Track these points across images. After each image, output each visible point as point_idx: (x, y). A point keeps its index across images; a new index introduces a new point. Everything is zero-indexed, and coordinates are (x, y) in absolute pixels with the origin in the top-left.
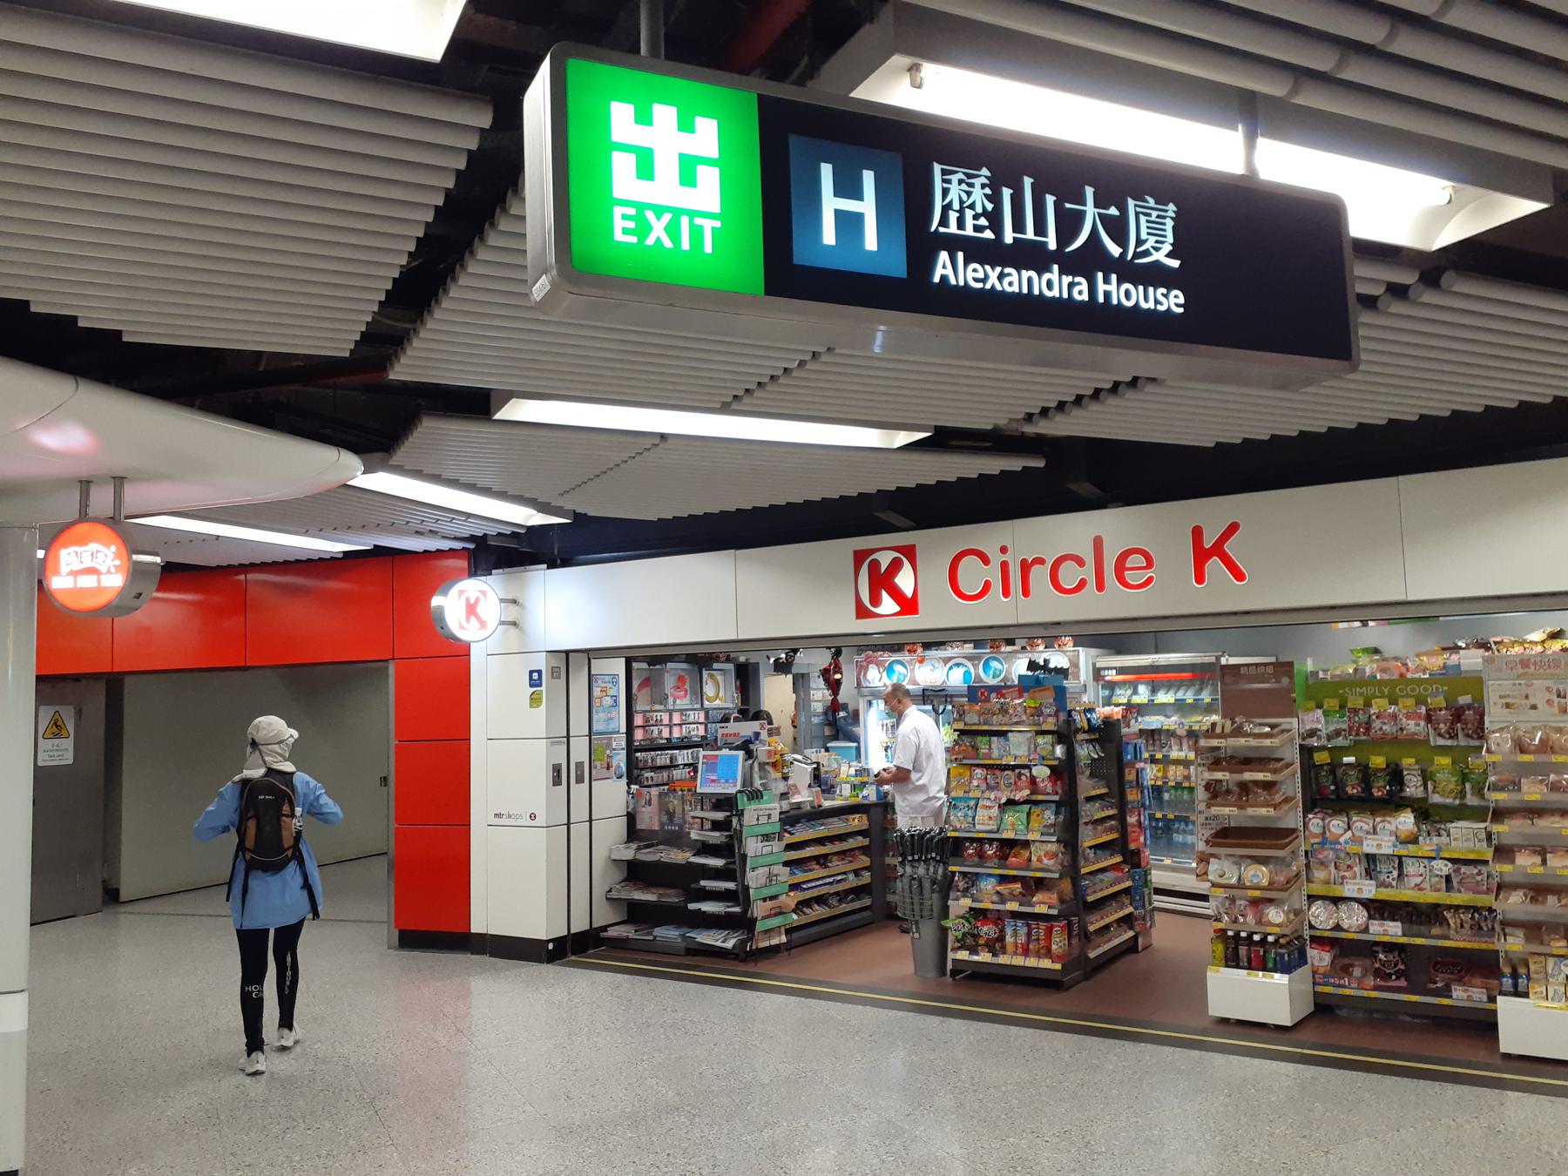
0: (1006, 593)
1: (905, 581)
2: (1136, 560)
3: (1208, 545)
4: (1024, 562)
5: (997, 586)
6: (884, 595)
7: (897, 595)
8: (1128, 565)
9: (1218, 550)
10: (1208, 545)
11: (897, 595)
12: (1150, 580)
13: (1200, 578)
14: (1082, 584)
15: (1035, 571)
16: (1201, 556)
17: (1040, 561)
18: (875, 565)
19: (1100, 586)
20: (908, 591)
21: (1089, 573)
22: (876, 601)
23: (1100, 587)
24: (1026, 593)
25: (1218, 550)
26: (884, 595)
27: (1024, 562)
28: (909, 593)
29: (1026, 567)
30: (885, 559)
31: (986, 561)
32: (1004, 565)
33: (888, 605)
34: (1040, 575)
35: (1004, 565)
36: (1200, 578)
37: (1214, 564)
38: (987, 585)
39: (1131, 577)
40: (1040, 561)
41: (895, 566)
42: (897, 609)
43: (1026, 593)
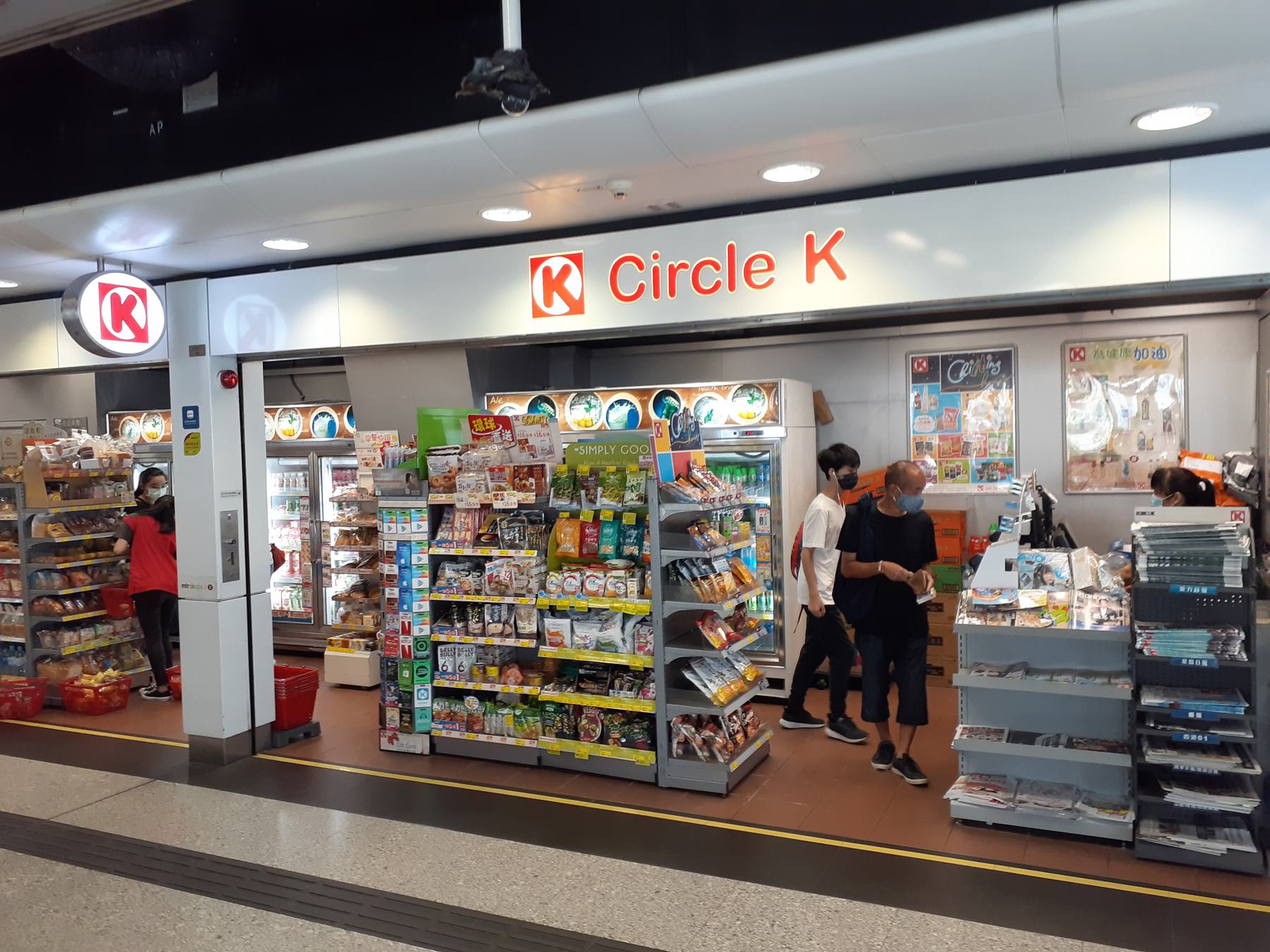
0: (656, 295)
1: (573, 284)
2: (761, 264)
3: (817, 250)
4: (671, 267)
6: (556, 297)
7: (566, 296)
8: (753, 269)
9: (825, 254)
10: (817, 250)
11: (566, 296)
12: (771, 281)
13: (810, 278)
14: (718, 285)
16: (812, 259)
17: (684, 266)
19: (732, 287)
22: (548, 302)
23: (732, 287)
24: (672, 293)
25: (825, 254)
26: (556, 297)
27: (671, 267)
29: (672, 271)
30: (556, 265)
31: (641, 266)
32: (656, 270)
33: (559, 305)
34: (684, 277)
35: (656, 270)
36: (810, 278)
37: (822, 267)
38: (642, 287)
39: (756, 279)
40: (684, 266)
41: (566, 271)
43: (672, 293)
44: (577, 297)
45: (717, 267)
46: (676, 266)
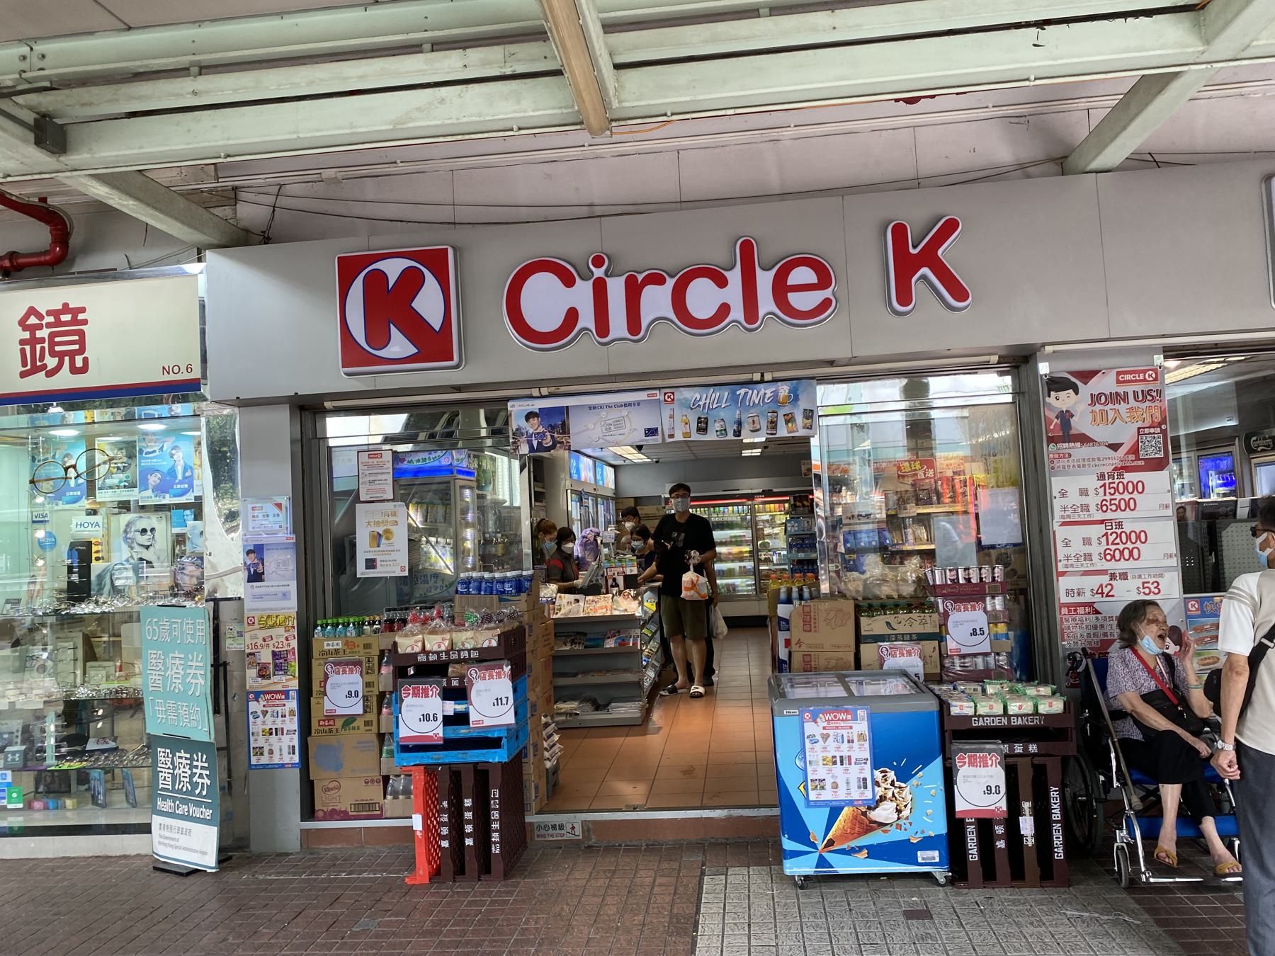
1: (429, 303)
5: (587, 319)
6: (393, 330)
7: (415, 327)
9: (929, 257)
12: (826, 304)
14: (724, 309)
17: (657, 279)
20: (436, 323)
21: (733, 293)
22: (378, 336)
26: (393, 330)
28: (437, 326)
31: (568, 281)
33: (399, 345)
34: (656, 301)
38: (572, 315)
42: (414, 350)
44: (437, 326)
45: (721, 282)
46: (640, 278)
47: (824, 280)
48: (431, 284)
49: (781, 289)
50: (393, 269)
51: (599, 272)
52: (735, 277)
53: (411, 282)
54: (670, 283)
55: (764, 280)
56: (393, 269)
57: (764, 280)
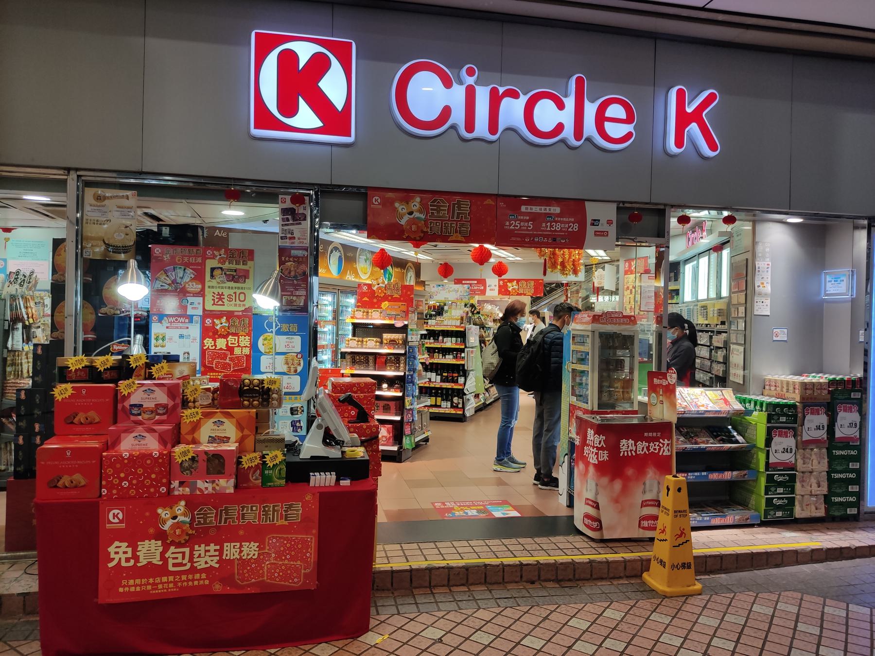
5: (458, 116)
6: (302, 104)
7: (321, 104)
11: (321, 104)
12: (629, 135)
14: (560, 127)
15: (506, 103)
17: (514, 95)
18: (288, 60)
20: (339, 102)
21: (567, 116)
22: (288, 107)
26: (302, 104)
27: (494, 92)
31: (447, 83)
38: (446, 112)
42: (317, 123)
45: (561, 106)
46: (501, 90)
47: (629, 120)
48: (336, 66)
49: (601, 119)
50: (305, 51)
51: (470, 80)
52: (570, 103)
53: (319, 65)
54: (523, 100)
55: (590, 110)
56: (305, 51)
57: (590, 110)
